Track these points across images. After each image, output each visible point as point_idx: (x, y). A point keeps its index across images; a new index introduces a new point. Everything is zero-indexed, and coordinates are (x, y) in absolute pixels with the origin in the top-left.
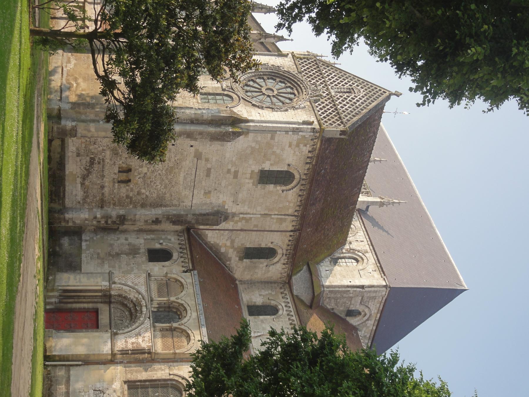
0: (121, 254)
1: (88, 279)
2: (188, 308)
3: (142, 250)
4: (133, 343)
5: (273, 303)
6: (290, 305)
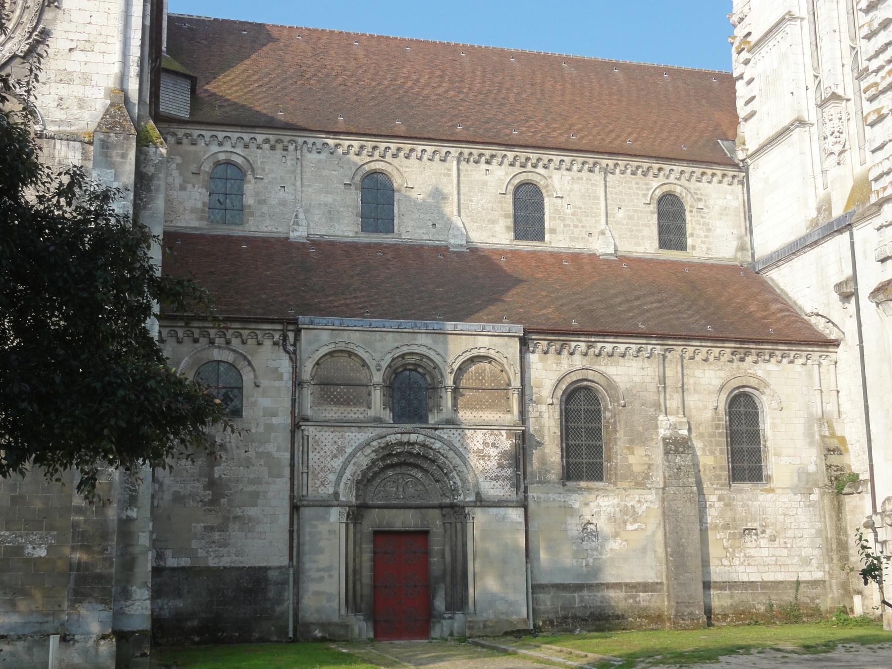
0: (210, 476)
1: (321, 551)
2: (405, 350)
5: (207, 167)
6: (221, 135)
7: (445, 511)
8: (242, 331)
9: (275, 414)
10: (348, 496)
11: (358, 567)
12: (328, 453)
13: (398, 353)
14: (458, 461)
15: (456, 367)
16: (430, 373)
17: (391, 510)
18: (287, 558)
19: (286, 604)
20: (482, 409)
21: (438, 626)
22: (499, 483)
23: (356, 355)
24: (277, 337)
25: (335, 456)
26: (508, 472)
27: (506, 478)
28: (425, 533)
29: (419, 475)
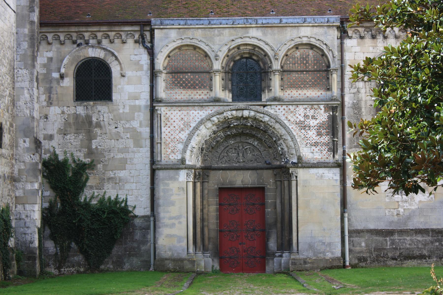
1: (173, 204)
2: (239, 42)
3: (81, 110)
4: (319, 134)
7: (276, 171)
8: (109, 33)
9: (136, 98)
10: (193, 159)
11: (205, 216)
12: (177, 127)
13: (234, 45)
14: (283, 131)
15: (281, 54)
16: (262, 60)
17: (233, 171)
18: (149, 209)
19: (149, 244)
20: (305, 87)
21: (271, 262)
22: (318, 148)
23: (200, 48)
24: (137, 36)
25: (182, 130)
26: (326, 139)
27: (324, 144)
28: (261, 190)
29: (256, 143)
